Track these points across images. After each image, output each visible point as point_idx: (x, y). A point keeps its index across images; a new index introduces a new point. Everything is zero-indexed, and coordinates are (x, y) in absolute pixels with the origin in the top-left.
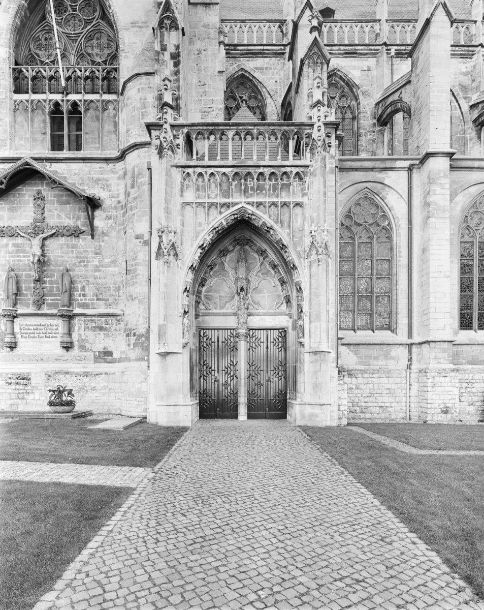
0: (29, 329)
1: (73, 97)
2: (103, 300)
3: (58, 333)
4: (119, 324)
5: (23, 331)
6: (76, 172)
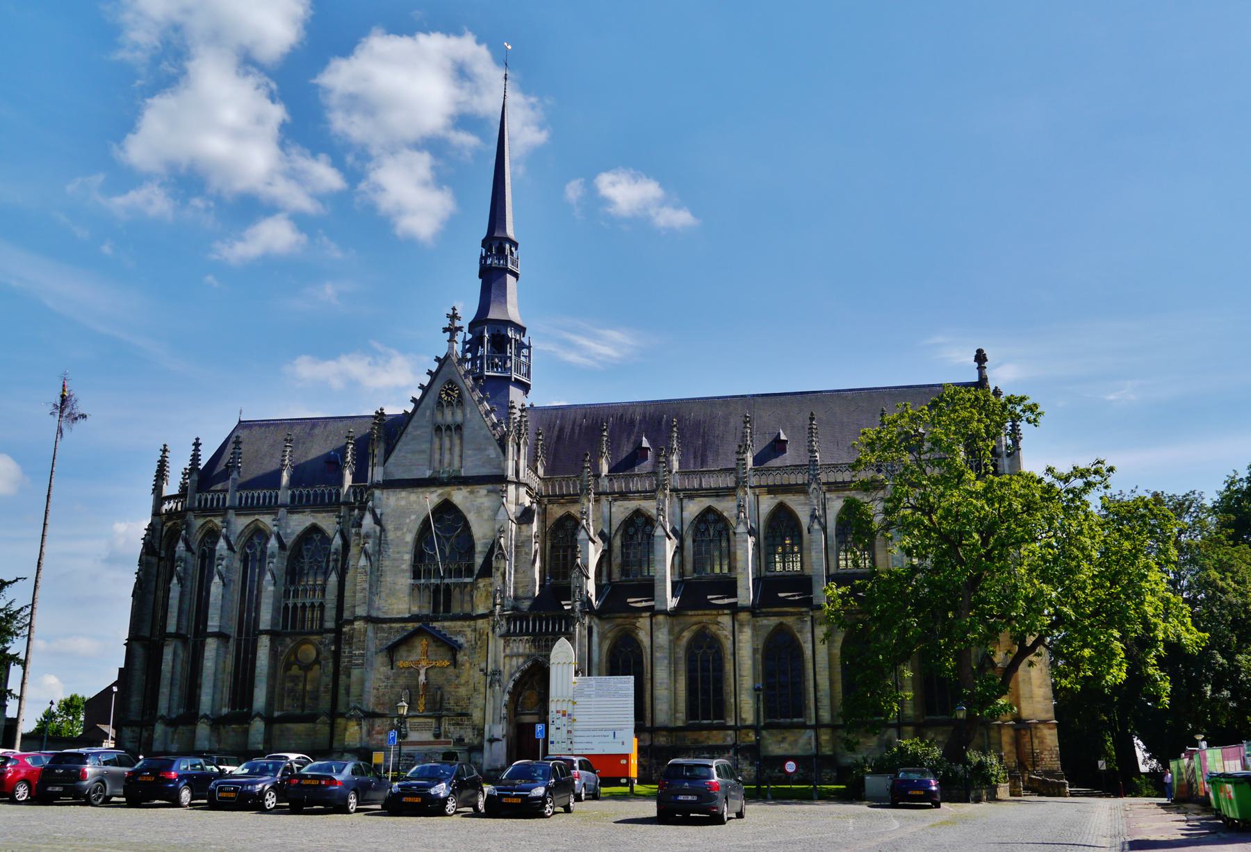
1: (446, 581)
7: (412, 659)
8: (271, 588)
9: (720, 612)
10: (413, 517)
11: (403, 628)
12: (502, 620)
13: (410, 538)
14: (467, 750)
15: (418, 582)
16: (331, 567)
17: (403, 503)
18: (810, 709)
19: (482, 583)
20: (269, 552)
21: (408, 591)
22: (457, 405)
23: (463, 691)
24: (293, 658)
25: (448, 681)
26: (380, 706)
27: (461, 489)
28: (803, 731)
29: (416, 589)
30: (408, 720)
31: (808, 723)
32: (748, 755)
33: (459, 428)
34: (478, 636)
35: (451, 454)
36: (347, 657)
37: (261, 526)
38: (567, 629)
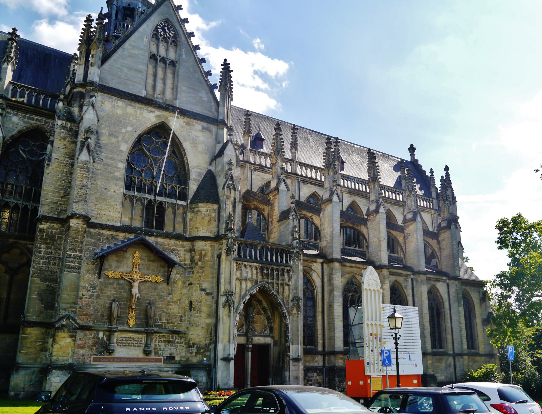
0: (122, 340)
2: (171, 323)
3: (142, 344)
4: (180, 339)
5: (119, 341)
6: (161, 243)
7: (121, 270)
10: (129, 129)
11: (113, 237)
13: (125, 148)
15: (131, 193)
17: (119, 112)
19: (203, 208)
21: (120, 200)
22: (171, 44)
23: (175, 309)
25: (160, 297)
29: (128, 202)
33: (173, 64)
35: (164, 84)
36: (43, 258)
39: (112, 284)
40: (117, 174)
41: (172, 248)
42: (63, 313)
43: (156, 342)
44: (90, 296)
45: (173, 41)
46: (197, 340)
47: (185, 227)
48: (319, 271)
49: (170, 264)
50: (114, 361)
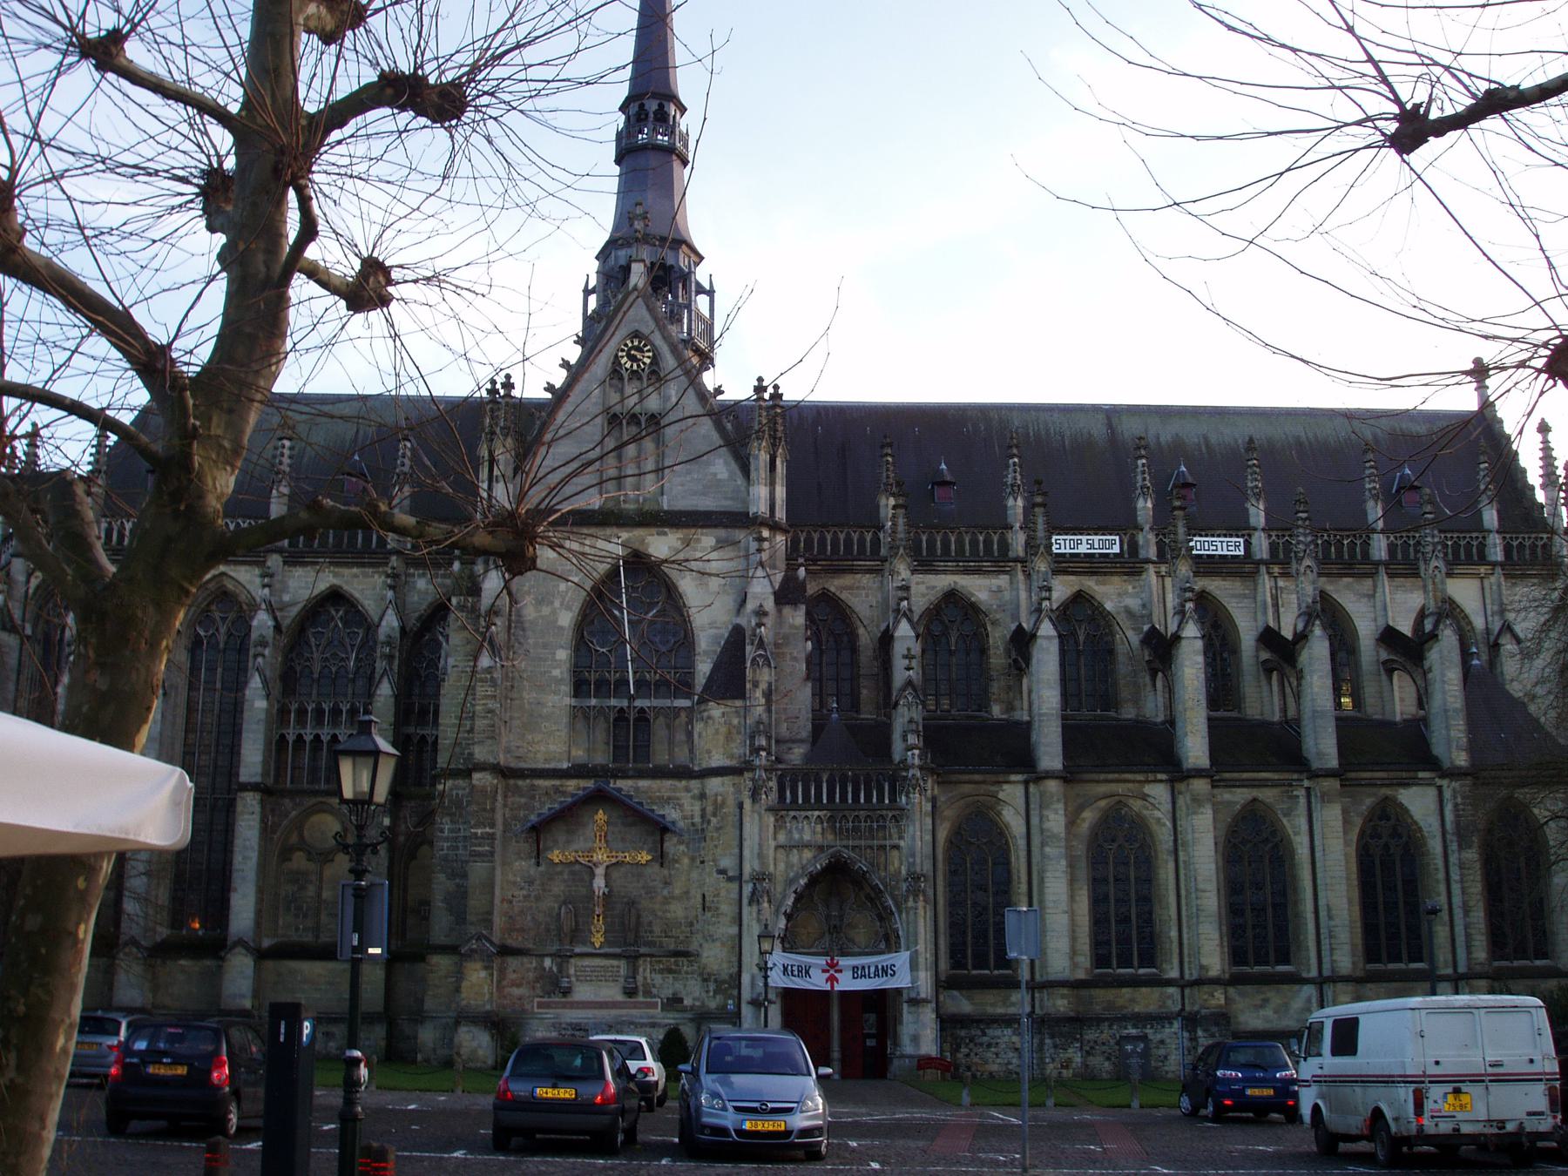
1: (638, 703)
7: (575, 846)
8: (261, 704)
9: (1151, 777)
11: (557, 790)
12: (770, 779)
13: (566, 619)
14: (692, 1020)
16: (379, 671)
18: (1307, 949)
19: (716, 710)
20: (254, 635)
21: (565, 720)
23: (677, 911)
24: (294, 839)
26: (515, 935)
27: (665, 534)
28: (1296, 987)
30: (572, 960)
31: (1305, 975)
32: (1214, 1029)
33: (655, 422)
34: (710, 809)
36: (447, 839)
37: (230, 586)
38: (893, 800)
39: (561, 873)
40: (556, 673)
41: (666, 795)
42: (473, 930)
43: (645, 972)
44: (525, 897)
45: (653, 372)
46: (716, 967)
47: (691, 751)
48: (1021, 802)
49: (662, 829)
50: (572, 1008)
